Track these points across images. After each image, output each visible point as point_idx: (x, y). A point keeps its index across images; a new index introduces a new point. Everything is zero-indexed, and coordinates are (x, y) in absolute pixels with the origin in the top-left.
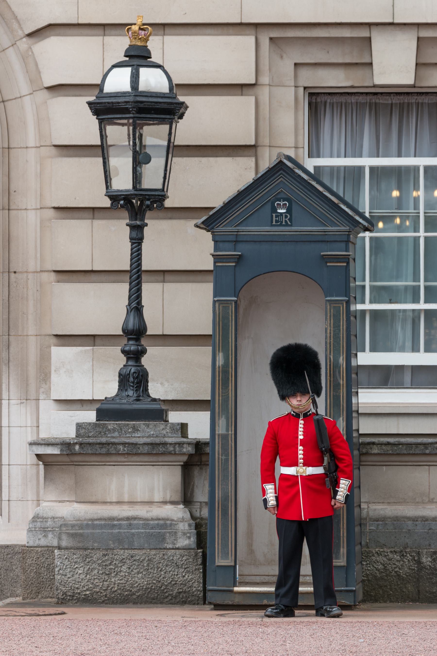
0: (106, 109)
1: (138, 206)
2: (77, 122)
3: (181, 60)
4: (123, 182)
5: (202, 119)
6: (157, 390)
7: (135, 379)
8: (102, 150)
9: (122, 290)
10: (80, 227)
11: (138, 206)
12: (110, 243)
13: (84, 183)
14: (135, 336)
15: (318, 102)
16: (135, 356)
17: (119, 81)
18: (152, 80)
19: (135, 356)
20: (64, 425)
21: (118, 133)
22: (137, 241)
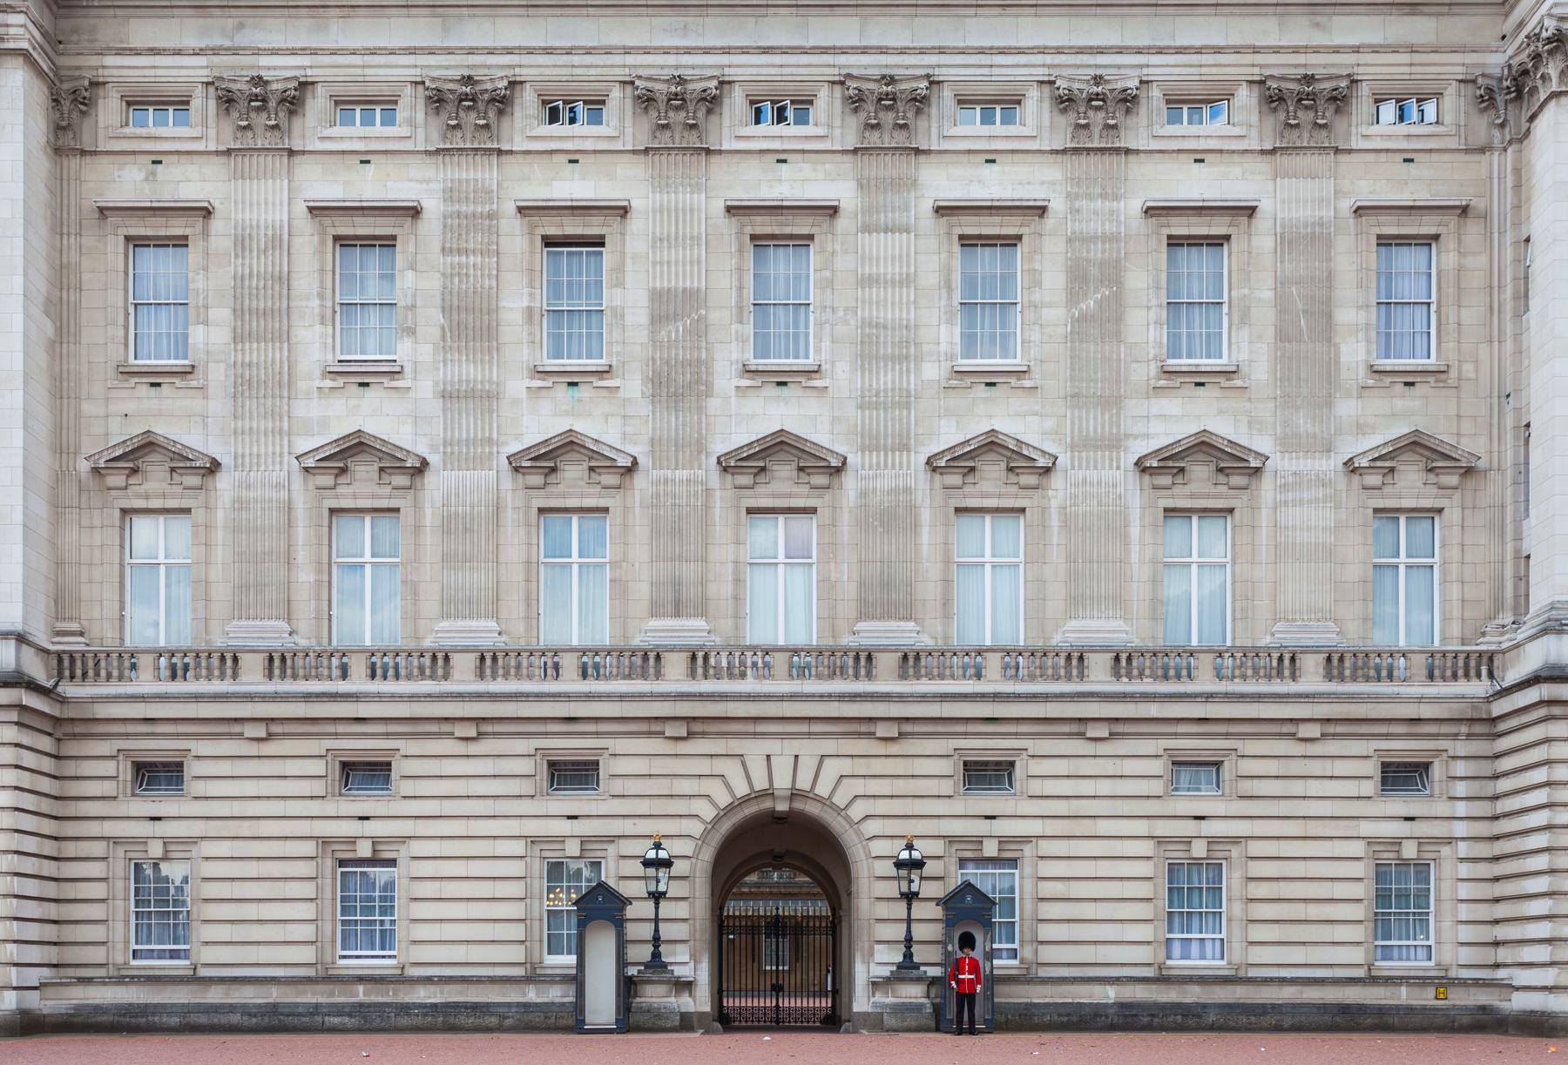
0: (900, 864)
1: (910, 897)
2: (888, 868)
3: (922, 849)
4: (905, 889)
5: (931, 868)
6: (915, 959)
7: (908, 955)
8: (898, 878)
9: (905, 925)
10: (884, 904)
11: (910, 897)
12: (900, 909)
13: (892, 889)
14: (909, 941)
15: (963, 862)
16: (909, 948)
17: (905, 855)
18: (916, 855)
19: (909, 948)
20: (886, 972)
21: (903, 873)
22: (909, 909)
